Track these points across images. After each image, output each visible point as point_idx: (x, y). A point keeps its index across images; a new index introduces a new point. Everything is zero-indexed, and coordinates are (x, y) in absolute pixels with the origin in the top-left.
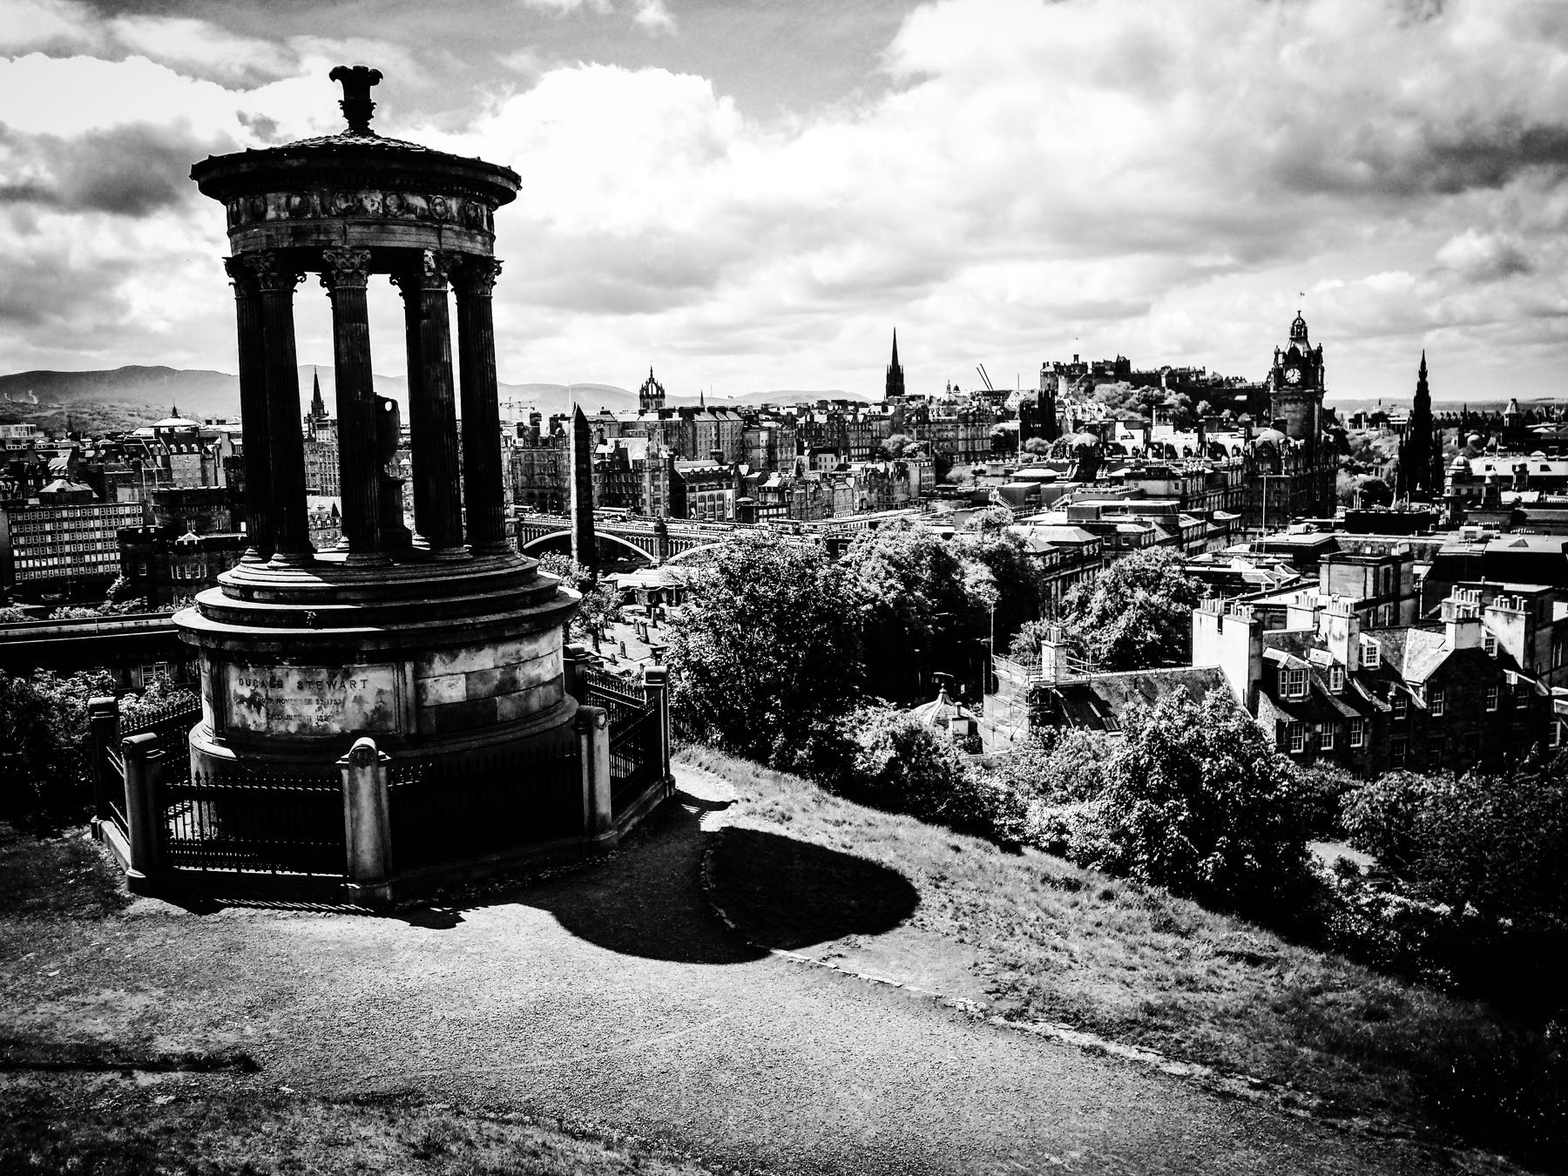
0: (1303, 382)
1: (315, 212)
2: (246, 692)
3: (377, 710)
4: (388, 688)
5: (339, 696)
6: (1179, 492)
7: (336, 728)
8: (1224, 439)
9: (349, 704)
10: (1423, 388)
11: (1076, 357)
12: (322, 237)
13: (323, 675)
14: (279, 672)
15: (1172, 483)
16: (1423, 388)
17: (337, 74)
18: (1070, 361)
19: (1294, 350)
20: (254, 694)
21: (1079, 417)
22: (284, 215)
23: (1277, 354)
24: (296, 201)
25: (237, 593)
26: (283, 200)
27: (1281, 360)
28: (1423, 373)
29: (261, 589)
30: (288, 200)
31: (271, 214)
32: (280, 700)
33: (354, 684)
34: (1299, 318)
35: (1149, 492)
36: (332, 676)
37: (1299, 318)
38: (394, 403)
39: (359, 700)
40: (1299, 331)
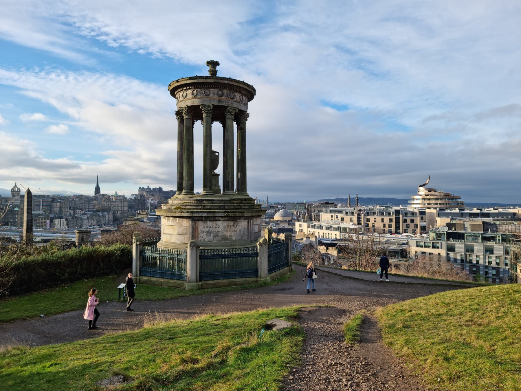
2: (207, 230)
3: (244, 234)
4: (246, 227)
5: (236, 230)
7: (234, 239)
9: (238, 232)
13: (231, 223)
22: (216, 96)
24: (220, 92)
25: (196, 202)
26: (216, 92)
29: (206, 200)
30: (218, 92)
31: (211, 95)
32: (218, 231)
33: (239, 226)
36: (234, 223)
39: (240, 231)
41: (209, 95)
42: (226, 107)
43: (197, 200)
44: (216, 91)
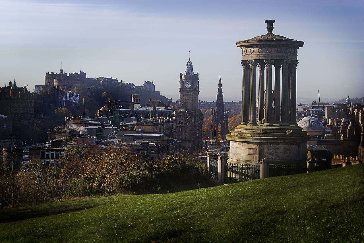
0: (192, 87)
1: (283, 52)
2: (270, 152)
6: (158, 131)
8: (162, 109)
9: (292, 153)
10: (220, 90)
11: (62, 71)
12: (283, 57)
13: (288, 147)
14: (278, 147)
15: (155, 127)
16: (220, 90)
17: (266, 22)
18: (59, 73)
19: (188, 74)
20: (272, 152)
21: (68, 98)
23: (181, 75)
24: (279, 50)
26: (276, 49)
27: (183, 78)
28: (220, 85)
30: (277, 49)
34: (190, 61)
35: (146, 131)
37: (190, 61)
38: (273, 91)
40: (190, 67)
41: (271, 52)
42: (284, 60)
43: (262, 130)
44: (276, 49)
